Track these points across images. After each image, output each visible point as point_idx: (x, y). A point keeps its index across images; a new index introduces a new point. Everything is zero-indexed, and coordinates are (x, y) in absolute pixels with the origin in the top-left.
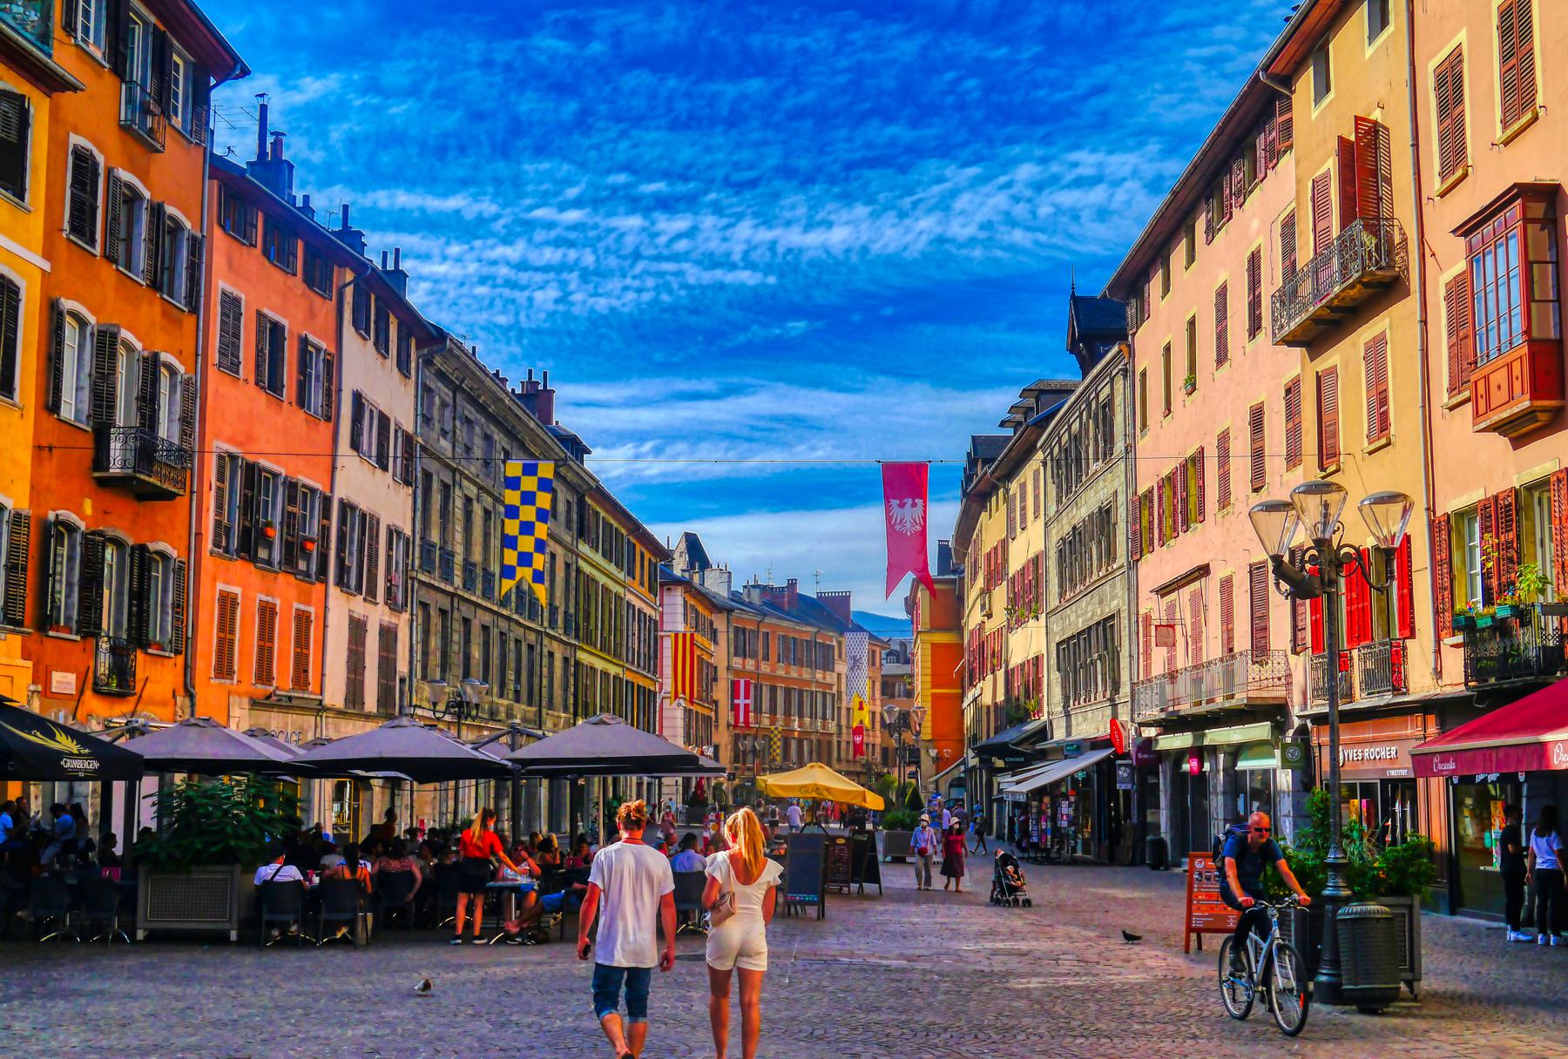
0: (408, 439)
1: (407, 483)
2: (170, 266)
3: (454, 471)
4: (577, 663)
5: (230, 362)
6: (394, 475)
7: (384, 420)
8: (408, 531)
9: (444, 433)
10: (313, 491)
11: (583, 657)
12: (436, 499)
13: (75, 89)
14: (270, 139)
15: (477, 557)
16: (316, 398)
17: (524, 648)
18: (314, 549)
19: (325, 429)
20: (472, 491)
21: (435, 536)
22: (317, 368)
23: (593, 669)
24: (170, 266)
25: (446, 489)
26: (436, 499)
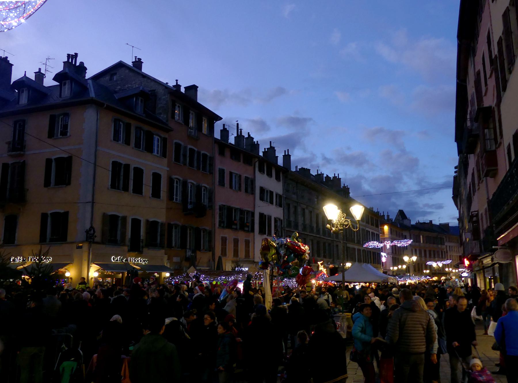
0: (280, 196)
1: (280, 206)
2: (205, 164)
3: (297, 203)
4: (347, 248)
5: (222, 183)
6: (276, 205)
7: (271, 193)
8: (282, 218)
9: (294, 194)
10: (249, 211)
11: (350, 245)
12: (292, 210)
13: (172, 131)
14: (239, 131)
15: (307, 222)
16: (249, 190)
17: (327, 244)
18: (249, 225)
19: (251, 197)
20: (305, 207)
21: (292, 219)
22: (249, 183)
23: (354, 249)
24: (205, 164)
25: (296, 208)
26: (292, 210)
